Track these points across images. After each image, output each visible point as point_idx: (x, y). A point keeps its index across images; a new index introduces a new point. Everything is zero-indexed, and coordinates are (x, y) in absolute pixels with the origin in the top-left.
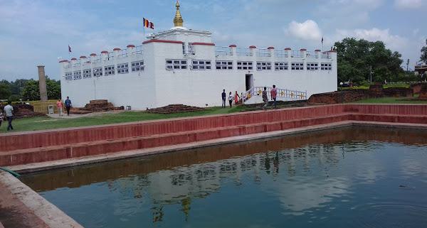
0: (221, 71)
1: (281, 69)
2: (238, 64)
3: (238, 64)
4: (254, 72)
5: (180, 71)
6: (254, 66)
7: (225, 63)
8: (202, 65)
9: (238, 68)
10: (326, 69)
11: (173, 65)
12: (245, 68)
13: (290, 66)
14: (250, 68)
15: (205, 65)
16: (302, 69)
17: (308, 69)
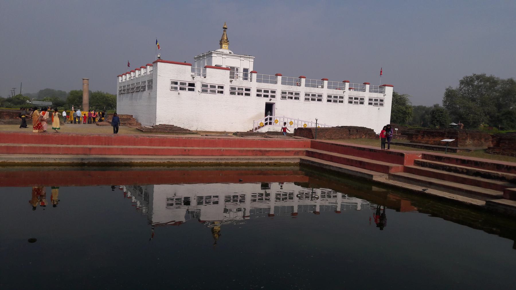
0: (236, 97)
1: (313, 100)
2: (258, 91)
3: (258, 91)
5: (186, 93)
6: (278, 95)
7: (242, 89)
8: (213, 89)
9: (258, 95)
10: (376, 104)
11: (177, 86)
12: (265, 96)
13: (325, 98)
14: (273, 97)
15: (217, 89)
16: (342, 102)
17: (350, 102)
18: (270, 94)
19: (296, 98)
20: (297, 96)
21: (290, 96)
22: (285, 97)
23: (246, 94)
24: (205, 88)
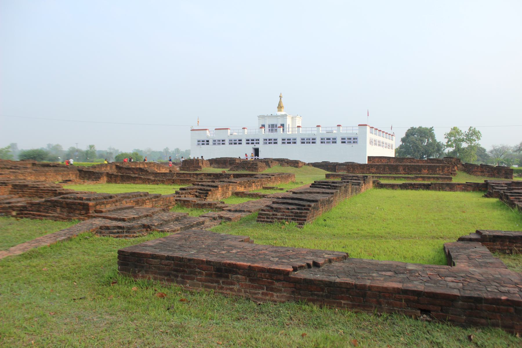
0: (233, 146)
4: (261, 147)
5: (205, 146)
6: (261, 141)
8: (219, 142)
14: (258, 143)
15: (221, 142)
18: (255, 142)
19: (275, 143)
20: (275, 141)
21: (270, 141)
22: (266, 143)
23: (239, 144)
24: (215, 142)
